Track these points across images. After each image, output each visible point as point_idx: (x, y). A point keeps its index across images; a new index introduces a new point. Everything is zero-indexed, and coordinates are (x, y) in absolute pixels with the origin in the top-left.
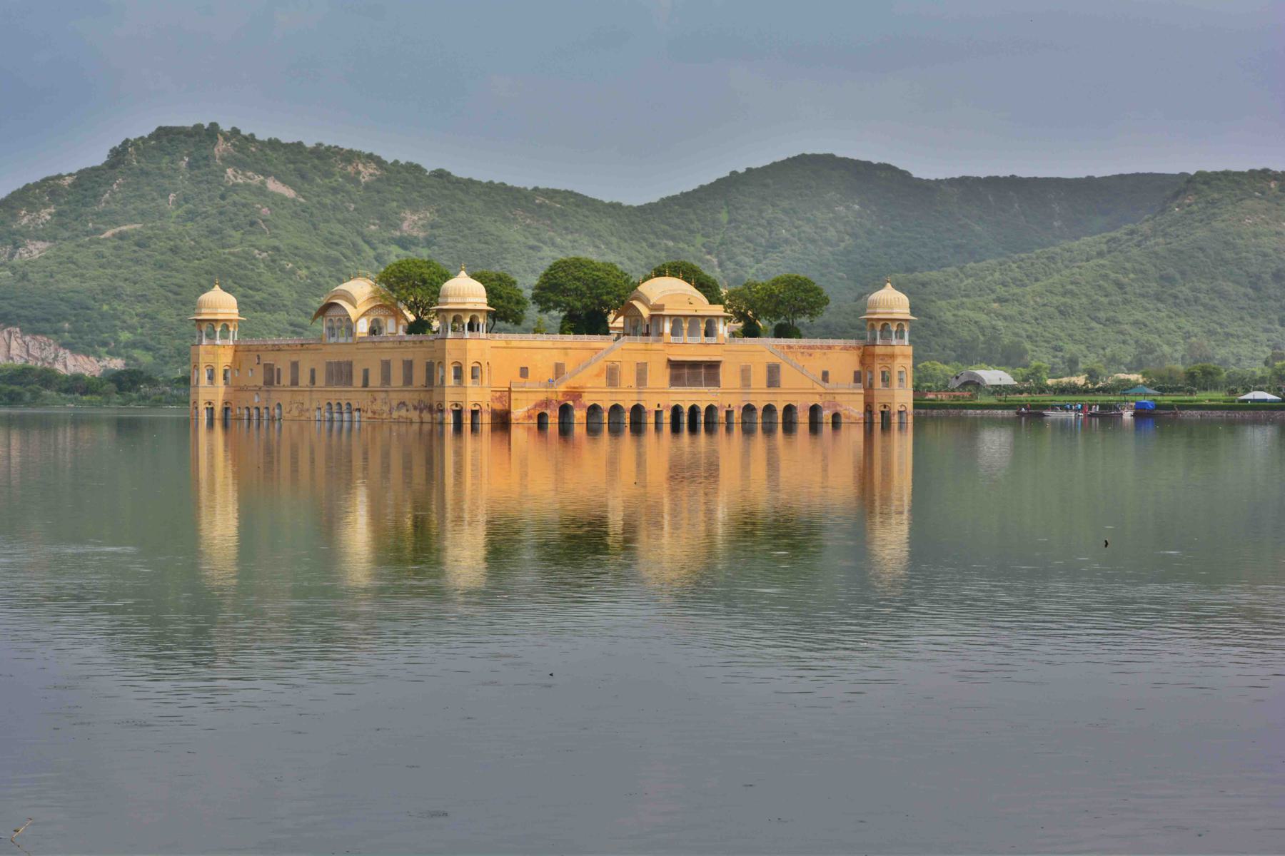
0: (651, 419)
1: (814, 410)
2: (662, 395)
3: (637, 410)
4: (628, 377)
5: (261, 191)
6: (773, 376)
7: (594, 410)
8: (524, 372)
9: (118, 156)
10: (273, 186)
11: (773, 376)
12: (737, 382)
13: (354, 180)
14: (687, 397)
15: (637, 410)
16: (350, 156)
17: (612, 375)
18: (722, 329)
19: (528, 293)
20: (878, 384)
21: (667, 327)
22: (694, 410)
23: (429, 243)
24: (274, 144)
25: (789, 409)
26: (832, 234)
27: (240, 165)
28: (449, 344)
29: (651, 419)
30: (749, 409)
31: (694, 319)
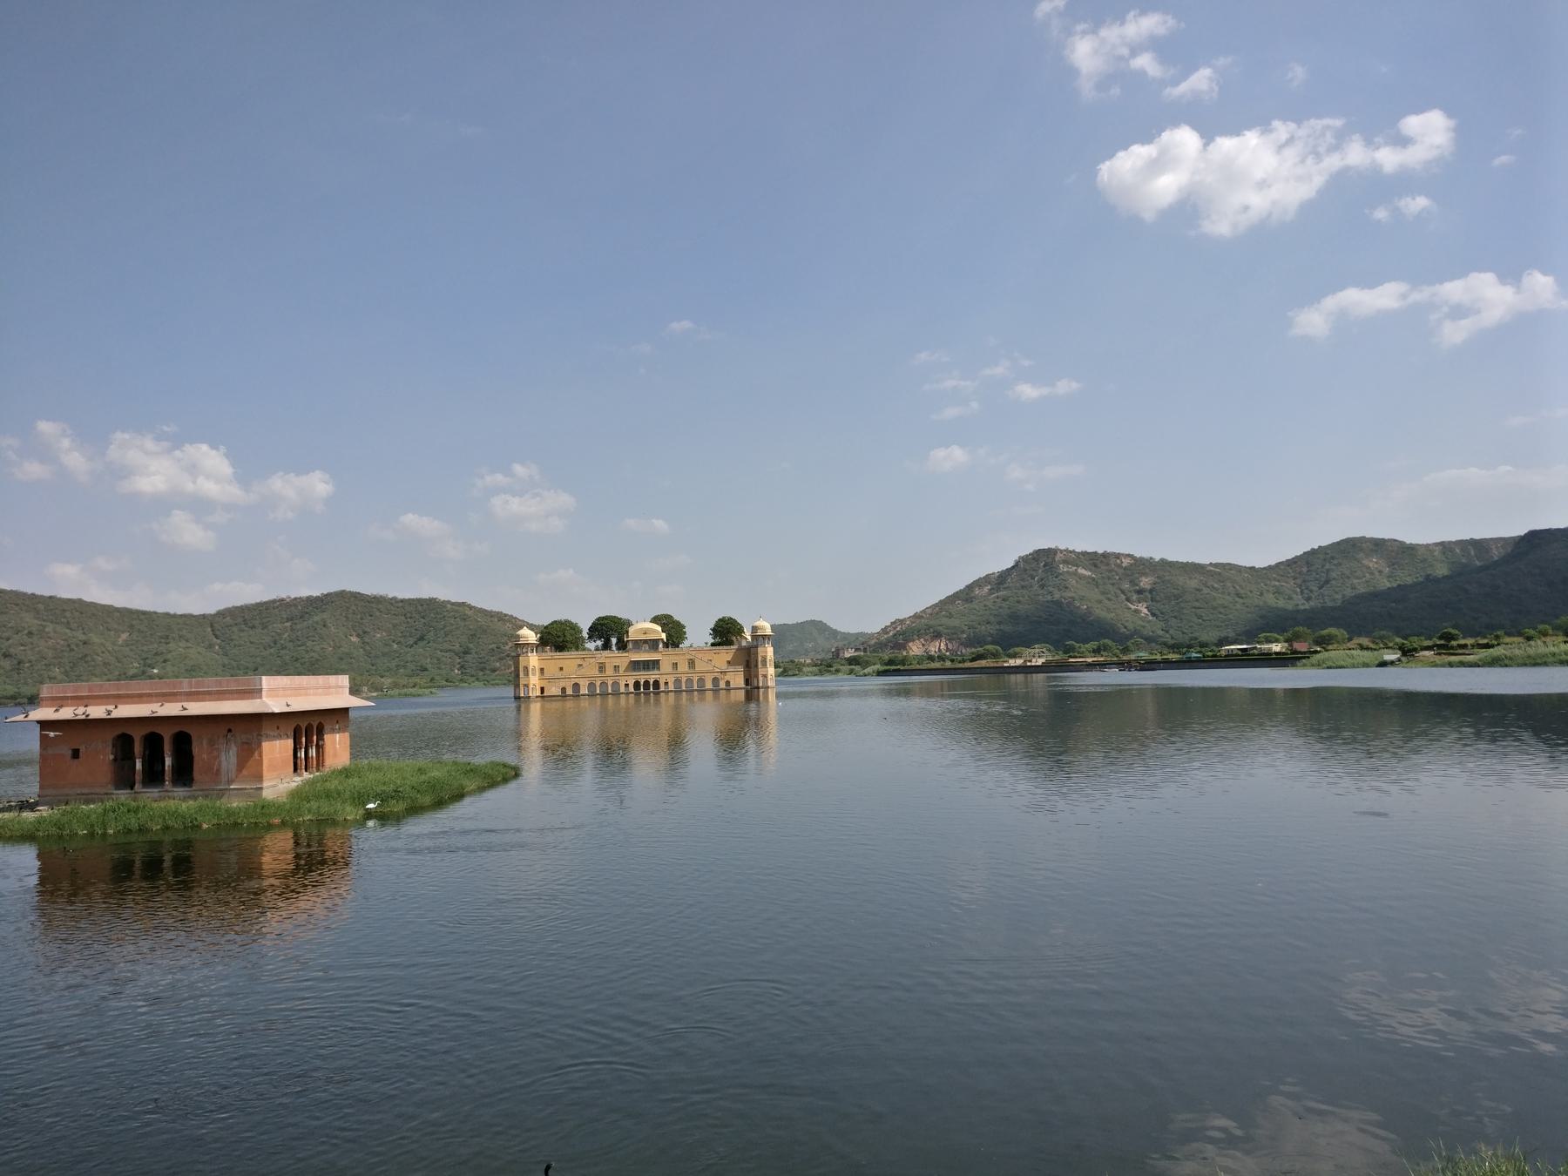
0: (622, 689)
1: (715, 681)
3: (616, 684)
4: (609, 671)
5: (1075, 573)
6: (692, 663)
9: (1017, 564)
10: (1081, 571)
11: (692, 663)
13: (1119, 566)
14: (642, 676)
16: (1118, 556)
17: (602, 668)
19: (585, 634)
21: (630, 646)
22: (647, 683)
23: (1151, 591)
24: (1085, 554)
26: (1359, 573)
27: (1065, 562)
29: (622, 689)
30: (678, 681)
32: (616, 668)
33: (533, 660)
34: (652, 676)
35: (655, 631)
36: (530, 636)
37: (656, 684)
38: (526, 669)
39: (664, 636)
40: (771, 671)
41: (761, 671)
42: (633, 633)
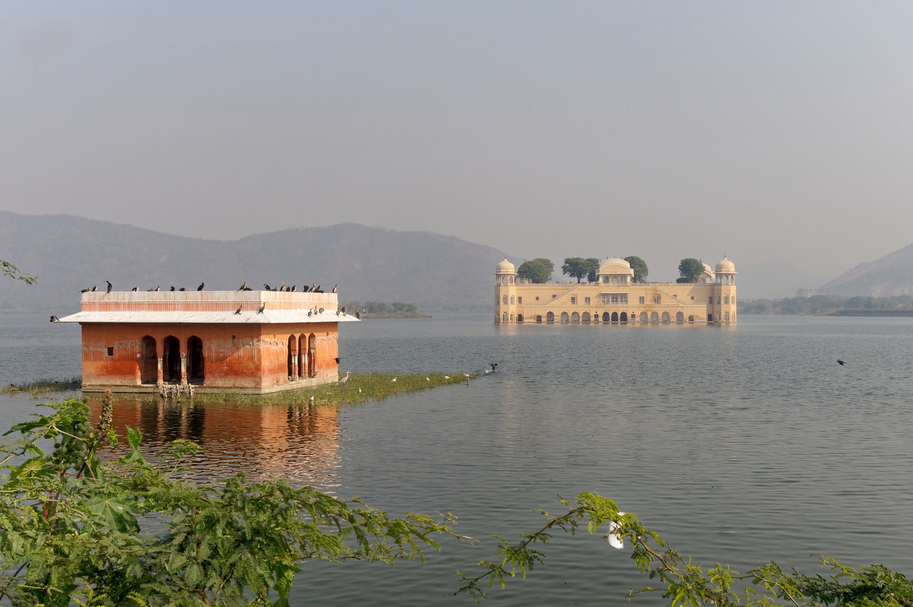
0: (592, 319)
2: (597, 309)
3: (586, 314)
4: (581, 301)
7: (564, 313)
8: (537, 299)
11: (657, 299)
12: (637, 302)
14: (611, 308)
15: (586, 314)
17: (573, 300)
18: (629, 279)
20: (716, 302)
22: (615, 314)
25: (666, 314)
28: (723, 287)
31: (615, 276)
32: (588, 300)
33: (512, 290)
34: (619, 308)
35: (624, 268)
36: (510, 268)
37: (624, 315)
38: (506, 298)
39: (632, 271)
40: (733, 308)
41: (724, 308)
42: (603, 270)
